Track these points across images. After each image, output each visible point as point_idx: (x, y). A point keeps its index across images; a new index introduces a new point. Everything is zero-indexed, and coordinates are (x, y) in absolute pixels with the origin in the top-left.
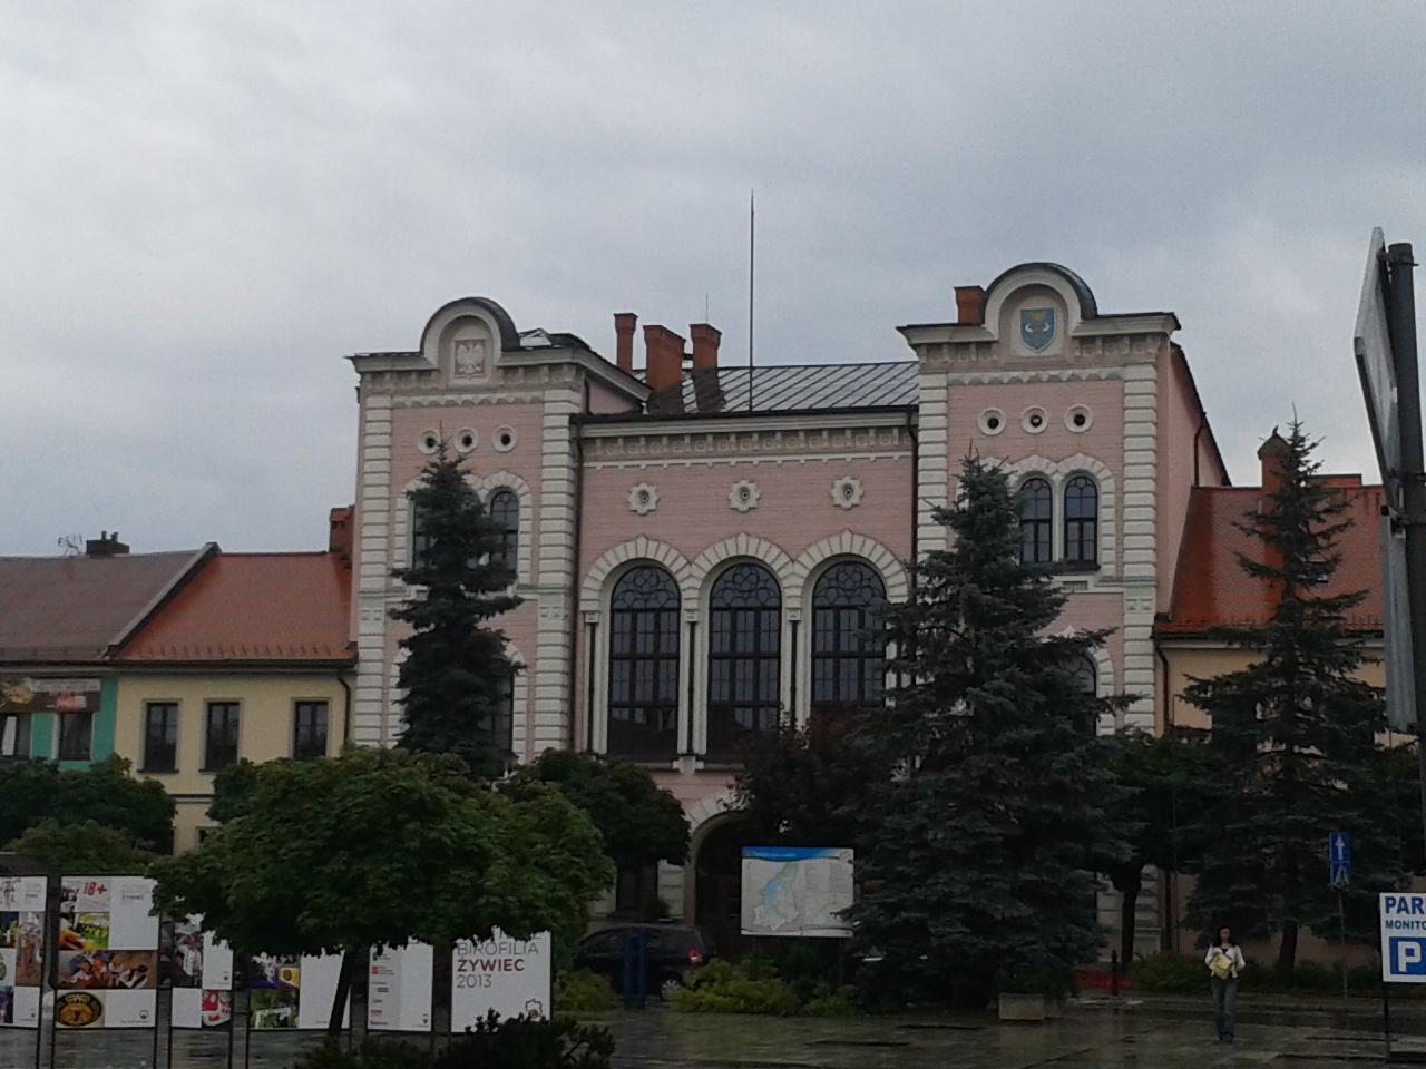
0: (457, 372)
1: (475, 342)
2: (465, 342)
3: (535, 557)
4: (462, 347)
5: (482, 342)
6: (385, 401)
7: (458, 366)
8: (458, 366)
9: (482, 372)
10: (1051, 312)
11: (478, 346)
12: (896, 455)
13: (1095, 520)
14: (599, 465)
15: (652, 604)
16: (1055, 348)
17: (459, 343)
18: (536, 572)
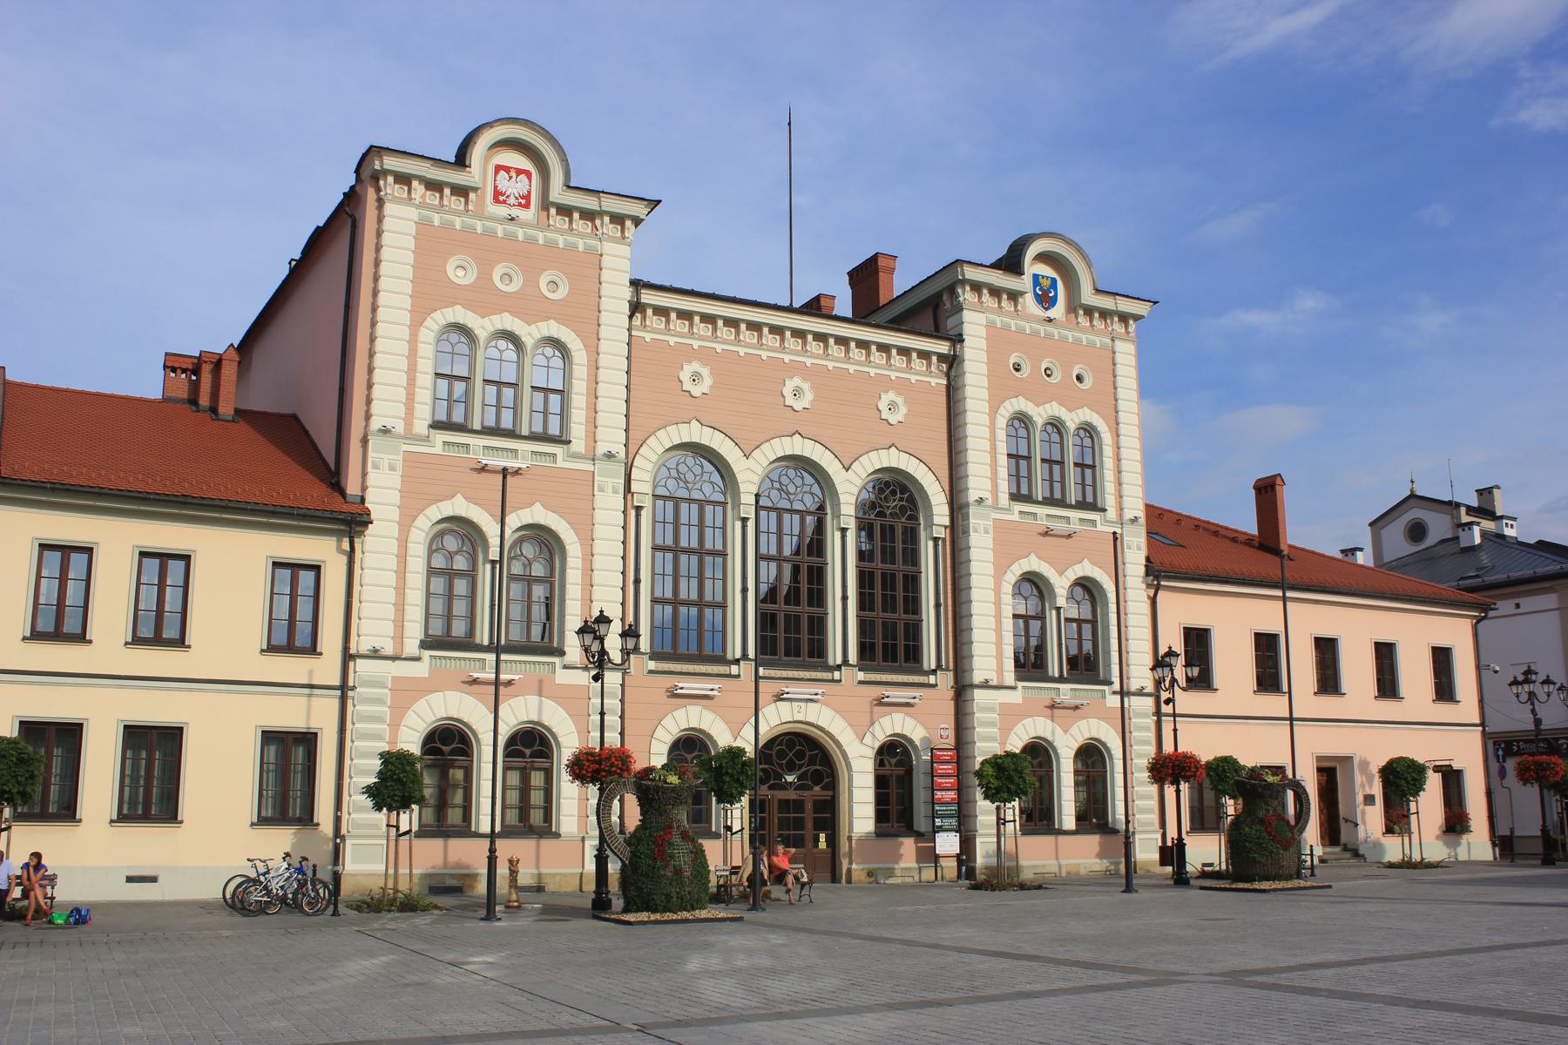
0: (496, 200)
1: (519, 172)
2: (507, 169)
3: (593, 424)
4: (502, 173)
5: (528, 174)
6: (413, 213)
7: (497, 194)
8: (497, 194)
9: (527, 206)
10: (1054, 280)
11: (523, 176)
12: (934, 381)
13: (1093, 467)
14: (648, 337)
15: (696, 495)
16: (1058, 311)
17: (498, 168)
18: (592, 439)
